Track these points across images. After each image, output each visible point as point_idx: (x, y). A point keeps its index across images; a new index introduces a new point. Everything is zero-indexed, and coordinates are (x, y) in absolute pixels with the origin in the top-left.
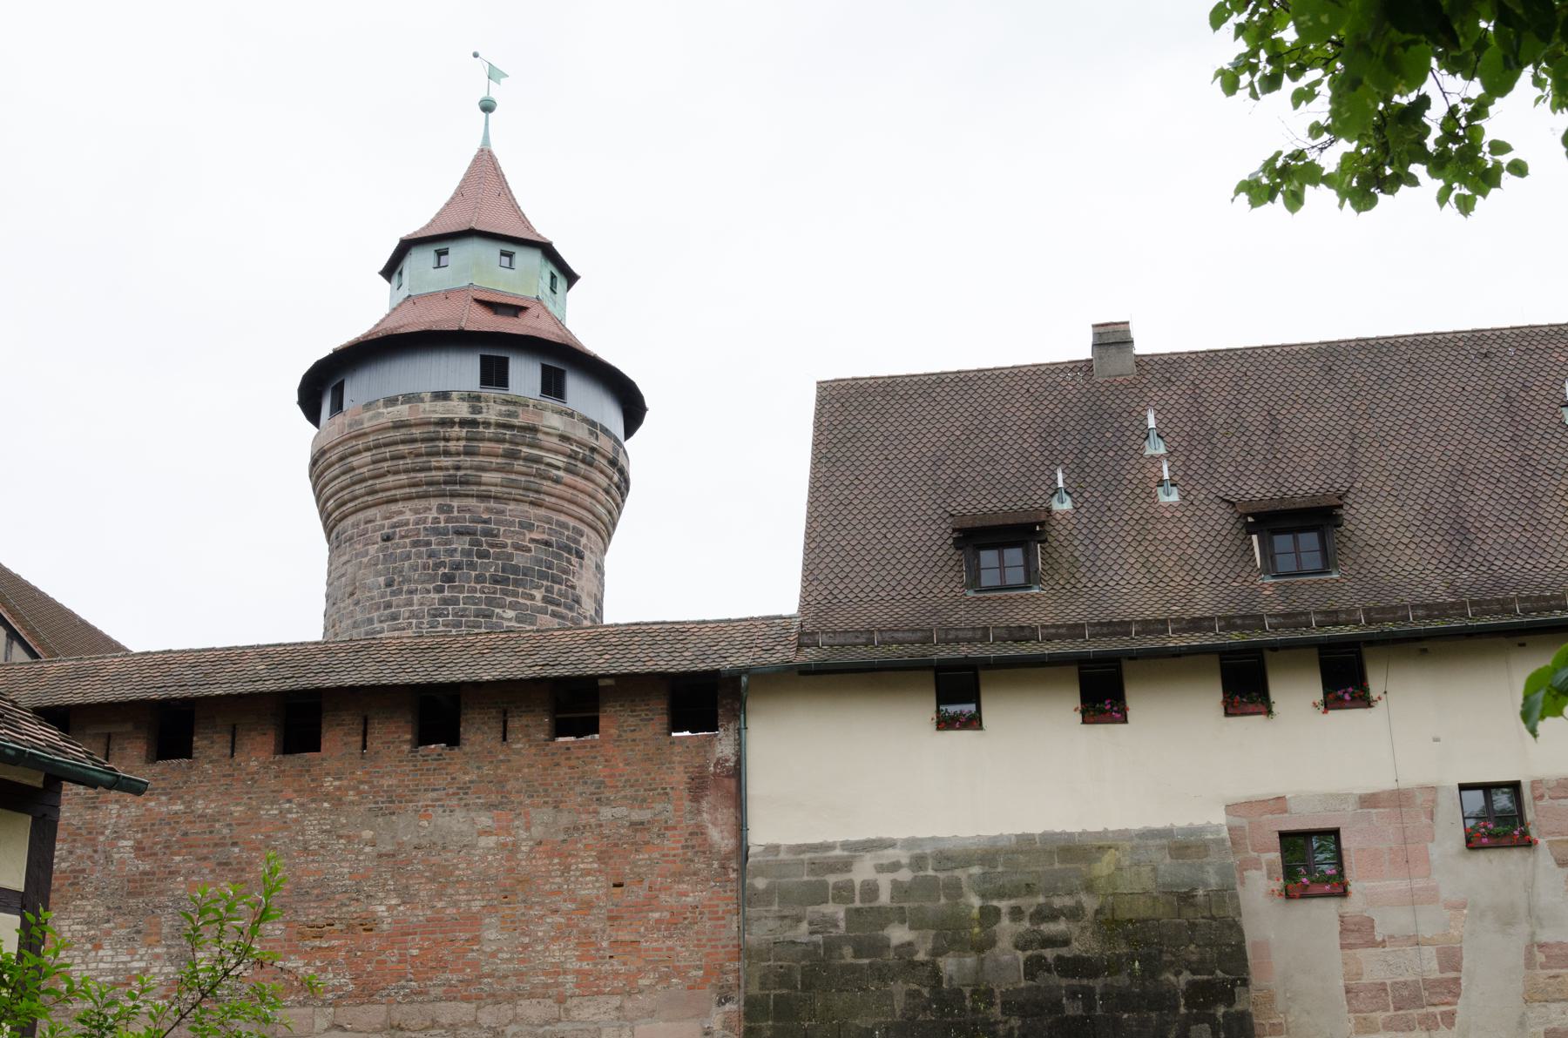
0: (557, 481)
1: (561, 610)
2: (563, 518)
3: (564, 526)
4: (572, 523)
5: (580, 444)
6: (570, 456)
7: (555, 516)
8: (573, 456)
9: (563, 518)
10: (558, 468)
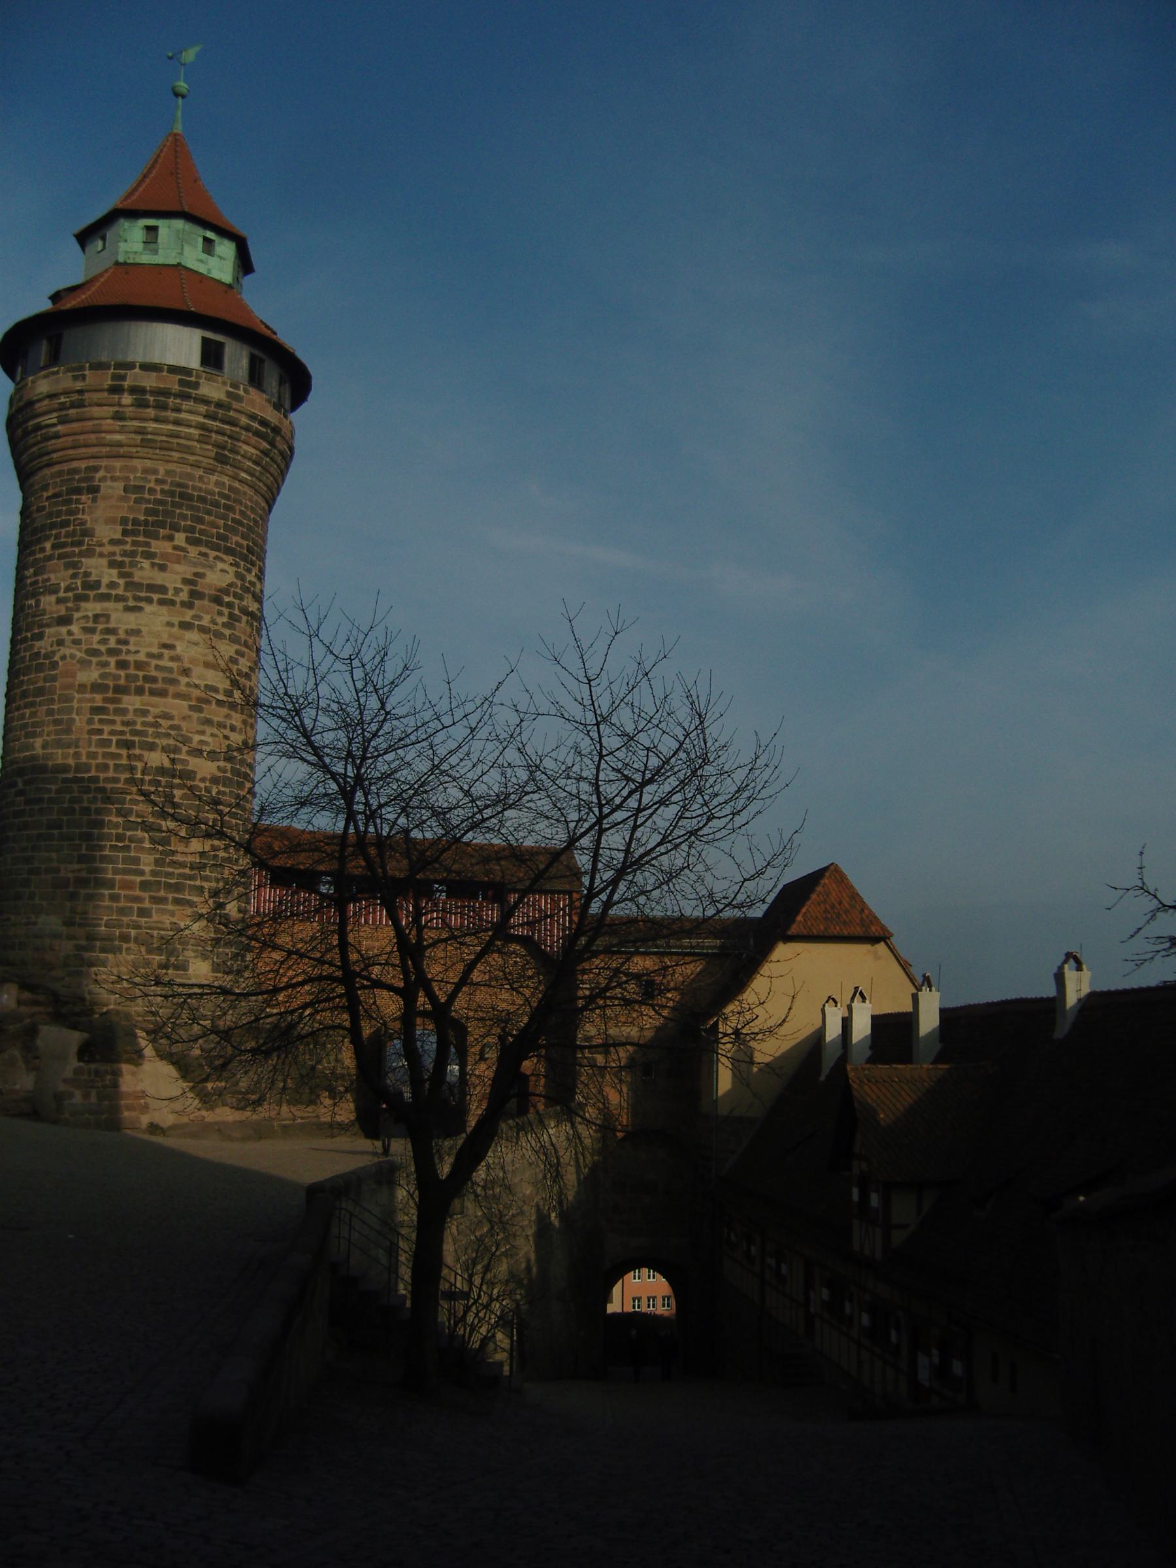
0: (57, 436)
1: (69, 549)
2: (75, 464)
3: (76, 471)
4: (83, 465)
5: (66, 393)
6: (61, 410)
7: (65, 467)
8: (63, 407)
9: (75, 464)
10: (54, 425)
